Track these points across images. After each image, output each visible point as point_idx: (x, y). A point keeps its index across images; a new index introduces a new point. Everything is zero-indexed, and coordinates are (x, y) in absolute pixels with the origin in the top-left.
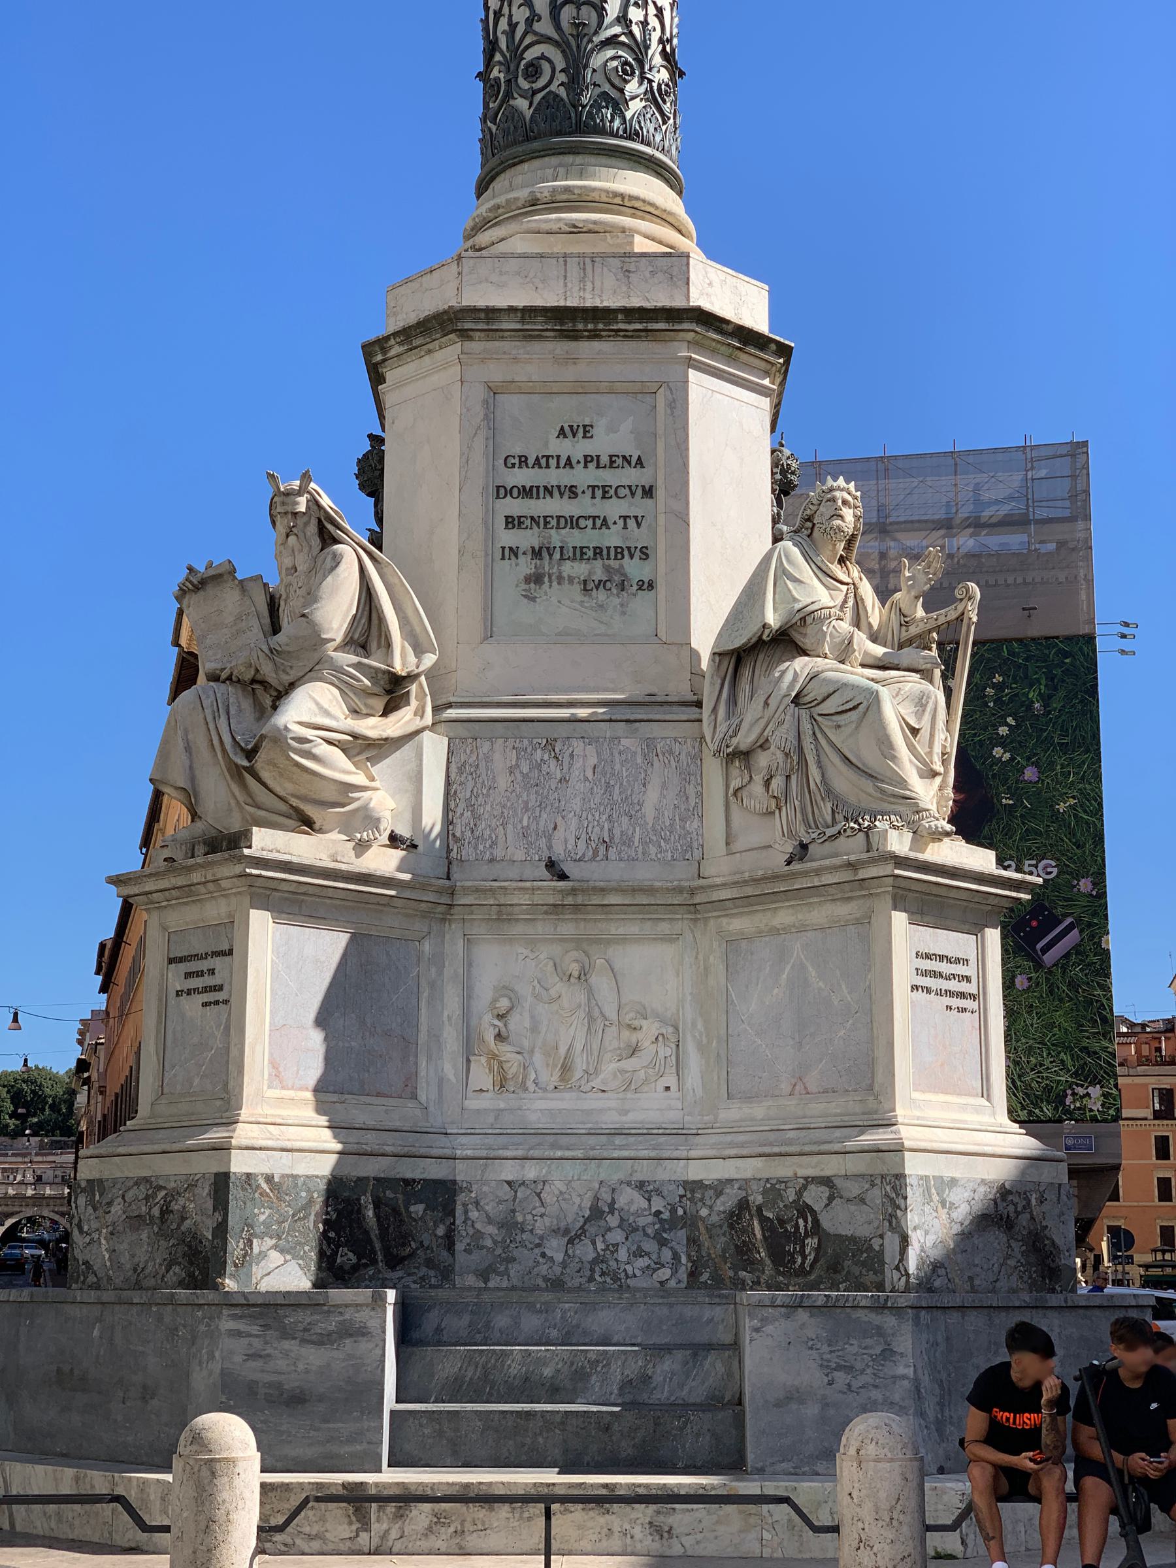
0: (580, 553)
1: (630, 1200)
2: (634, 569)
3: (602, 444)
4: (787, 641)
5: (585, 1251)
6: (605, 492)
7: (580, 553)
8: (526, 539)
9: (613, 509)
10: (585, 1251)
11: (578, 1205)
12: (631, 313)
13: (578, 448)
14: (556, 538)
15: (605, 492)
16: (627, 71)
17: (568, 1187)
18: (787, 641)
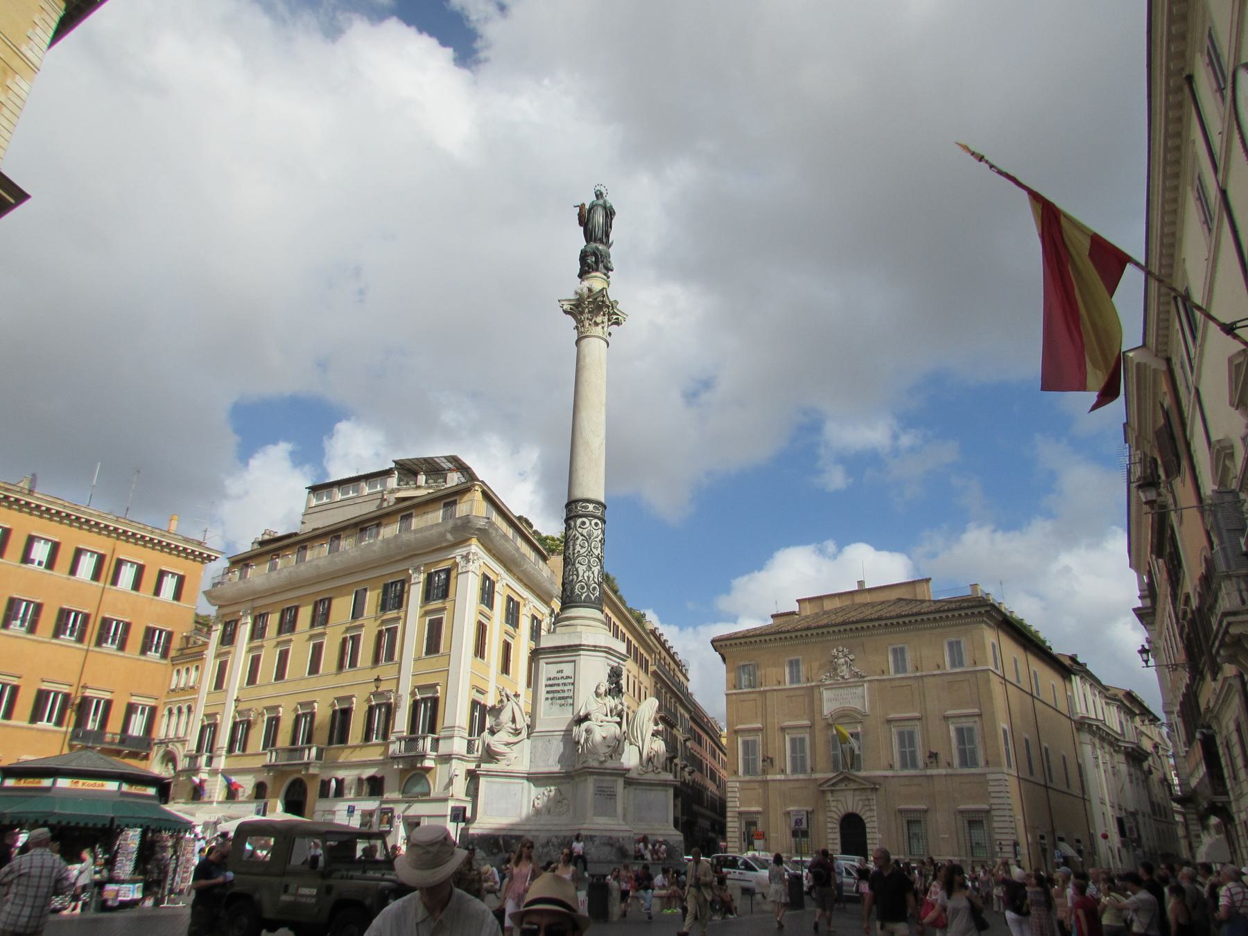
0: (560, 698)
1: (554, 840)
2: (570, 701)
3: (564, 674)
4: (586, 718)
5: (545, 850)
6: (565, 684)
7: (560, 698)
8: (550, 696)
9: (566, 688)
10: (545, 850)
11: (544, 841)
12: (569, 646)
13: (560, 675)
14: (557, 695)
15: (565, 684)
16: (583, 588)
17: (543, 837)
18: (586, 718)
